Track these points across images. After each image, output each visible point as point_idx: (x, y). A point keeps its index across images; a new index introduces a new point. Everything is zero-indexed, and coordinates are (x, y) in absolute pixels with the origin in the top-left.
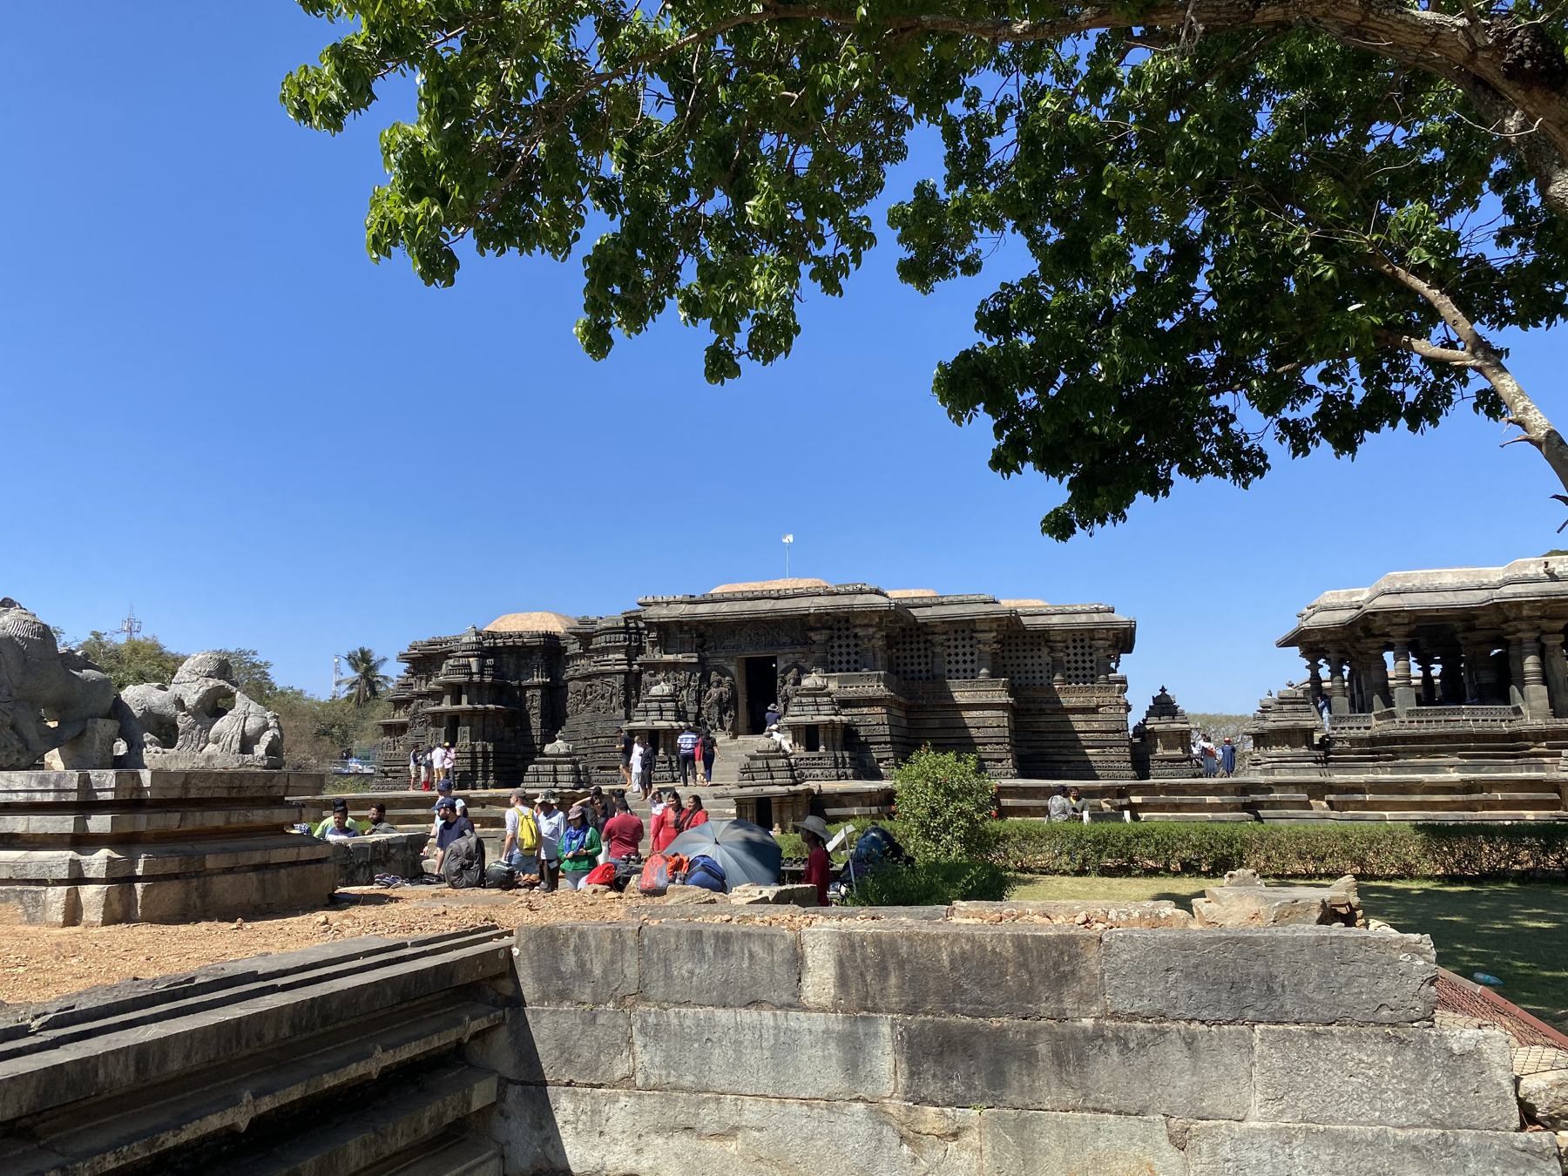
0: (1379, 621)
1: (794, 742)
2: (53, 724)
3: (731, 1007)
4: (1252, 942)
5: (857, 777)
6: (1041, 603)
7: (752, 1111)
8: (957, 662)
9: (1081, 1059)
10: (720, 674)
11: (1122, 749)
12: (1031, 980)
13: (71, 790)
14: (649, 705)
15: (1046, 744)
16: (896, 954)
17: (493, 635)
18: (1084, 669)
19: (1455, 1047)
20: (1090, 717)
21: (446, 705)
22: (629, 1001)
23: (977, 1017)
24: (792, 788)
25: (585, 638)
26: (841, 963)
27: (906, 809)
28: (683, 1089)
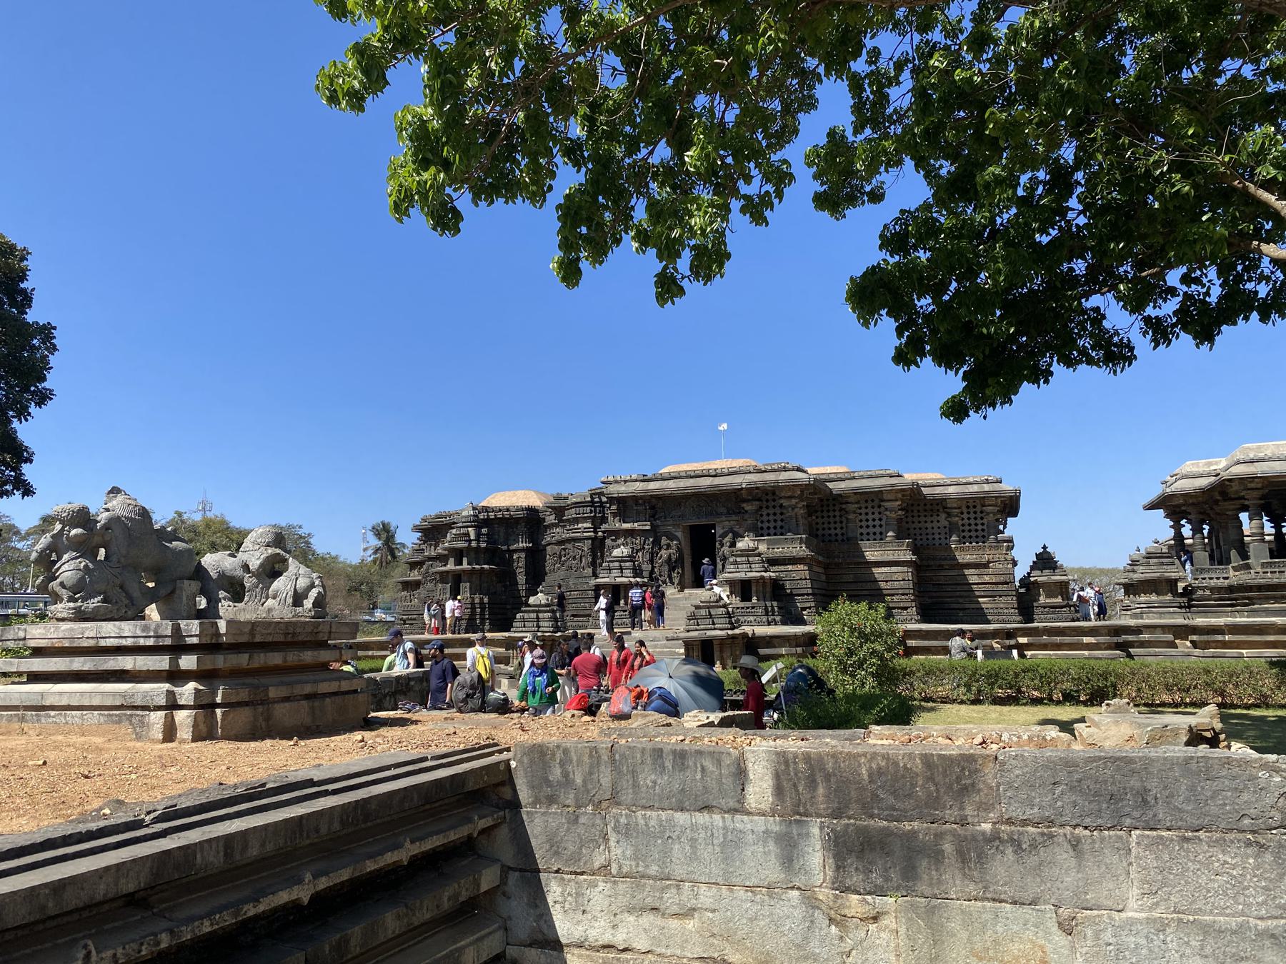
0: (1235, 487)
2: (151, 585)
3: (688, 811)
4: (1128, 761)
5: (784, 623)
6: (939, 476)
7: (706, 896)
8: (868, 527)
9: (981, 857)
10: (668, 538)
11: (1010, 598)
12: (938, 791)
13: (166, 636)
14: (611, 565)
16: (823, 769)
17: (486, 509)
18: (977, 530)
21: (451, 566)
22: (604, 805)
23: (892, 821)
24: (730, 632)
25: (559, 511)
26: (777, 776)
27: (826, 649)
28: (649, 877)
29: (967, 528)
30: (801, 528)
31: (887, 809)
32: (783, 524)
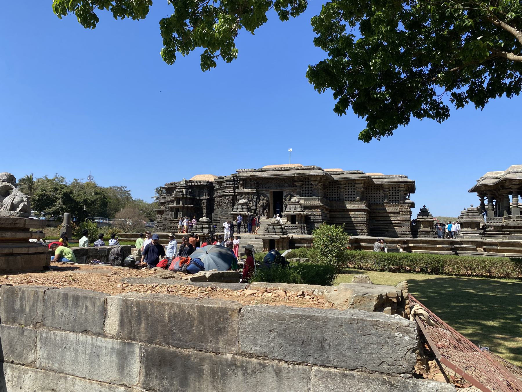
0: (507, 183)
1: (287, 221)
3: (77, 332)
4: (315, 319)
6: (381, 174)
8: (349, 195)
9: (224, 375)
10: (263, 196)
11: (408, 227)
12: (204, 330)
14: (238, 206)
15: (380, 224)
16: (145, 312)
17: (191, 182)
18: (395, 198)
21: (175, 205)
22: (38, 325)
23: (178, 348)
24: (282, 236)
25: (220, 183)
26: (122, 315)
29: (391, 197)
30: (320, 194)
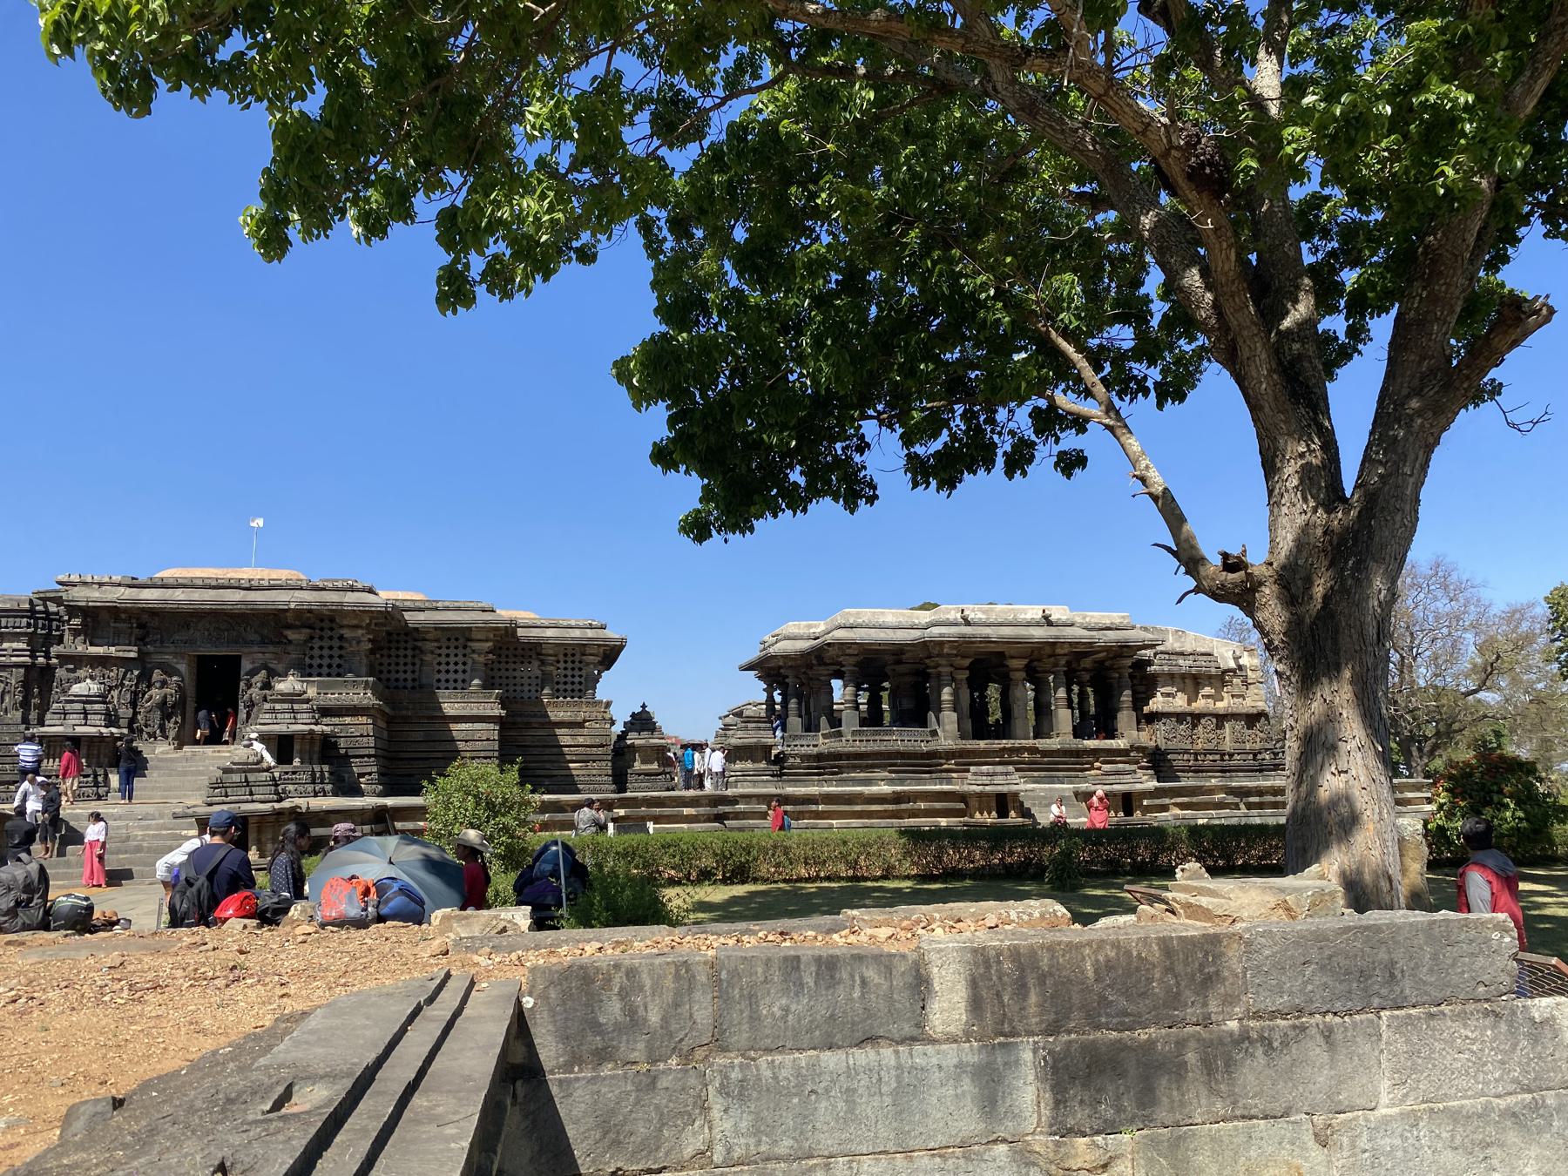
0: (832, 652)
3: (839, 1048)
5: (335, 794)
6: (532, 615)
8: (448, 672)
9: (1229, 1064)
10: (165, 673)
11: (604, 763)
12: (1178, 984)
14: (68, 706)
18: (573, 683)
19: (1536, 1015)
20: (576, 731)
24: (277, 806)
26: (973, 984)
28: (778, 1159)
31: (1117, 1016)
32: (341, 662)
